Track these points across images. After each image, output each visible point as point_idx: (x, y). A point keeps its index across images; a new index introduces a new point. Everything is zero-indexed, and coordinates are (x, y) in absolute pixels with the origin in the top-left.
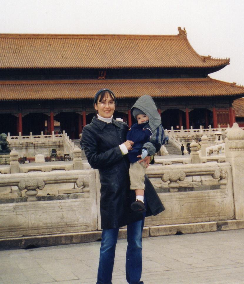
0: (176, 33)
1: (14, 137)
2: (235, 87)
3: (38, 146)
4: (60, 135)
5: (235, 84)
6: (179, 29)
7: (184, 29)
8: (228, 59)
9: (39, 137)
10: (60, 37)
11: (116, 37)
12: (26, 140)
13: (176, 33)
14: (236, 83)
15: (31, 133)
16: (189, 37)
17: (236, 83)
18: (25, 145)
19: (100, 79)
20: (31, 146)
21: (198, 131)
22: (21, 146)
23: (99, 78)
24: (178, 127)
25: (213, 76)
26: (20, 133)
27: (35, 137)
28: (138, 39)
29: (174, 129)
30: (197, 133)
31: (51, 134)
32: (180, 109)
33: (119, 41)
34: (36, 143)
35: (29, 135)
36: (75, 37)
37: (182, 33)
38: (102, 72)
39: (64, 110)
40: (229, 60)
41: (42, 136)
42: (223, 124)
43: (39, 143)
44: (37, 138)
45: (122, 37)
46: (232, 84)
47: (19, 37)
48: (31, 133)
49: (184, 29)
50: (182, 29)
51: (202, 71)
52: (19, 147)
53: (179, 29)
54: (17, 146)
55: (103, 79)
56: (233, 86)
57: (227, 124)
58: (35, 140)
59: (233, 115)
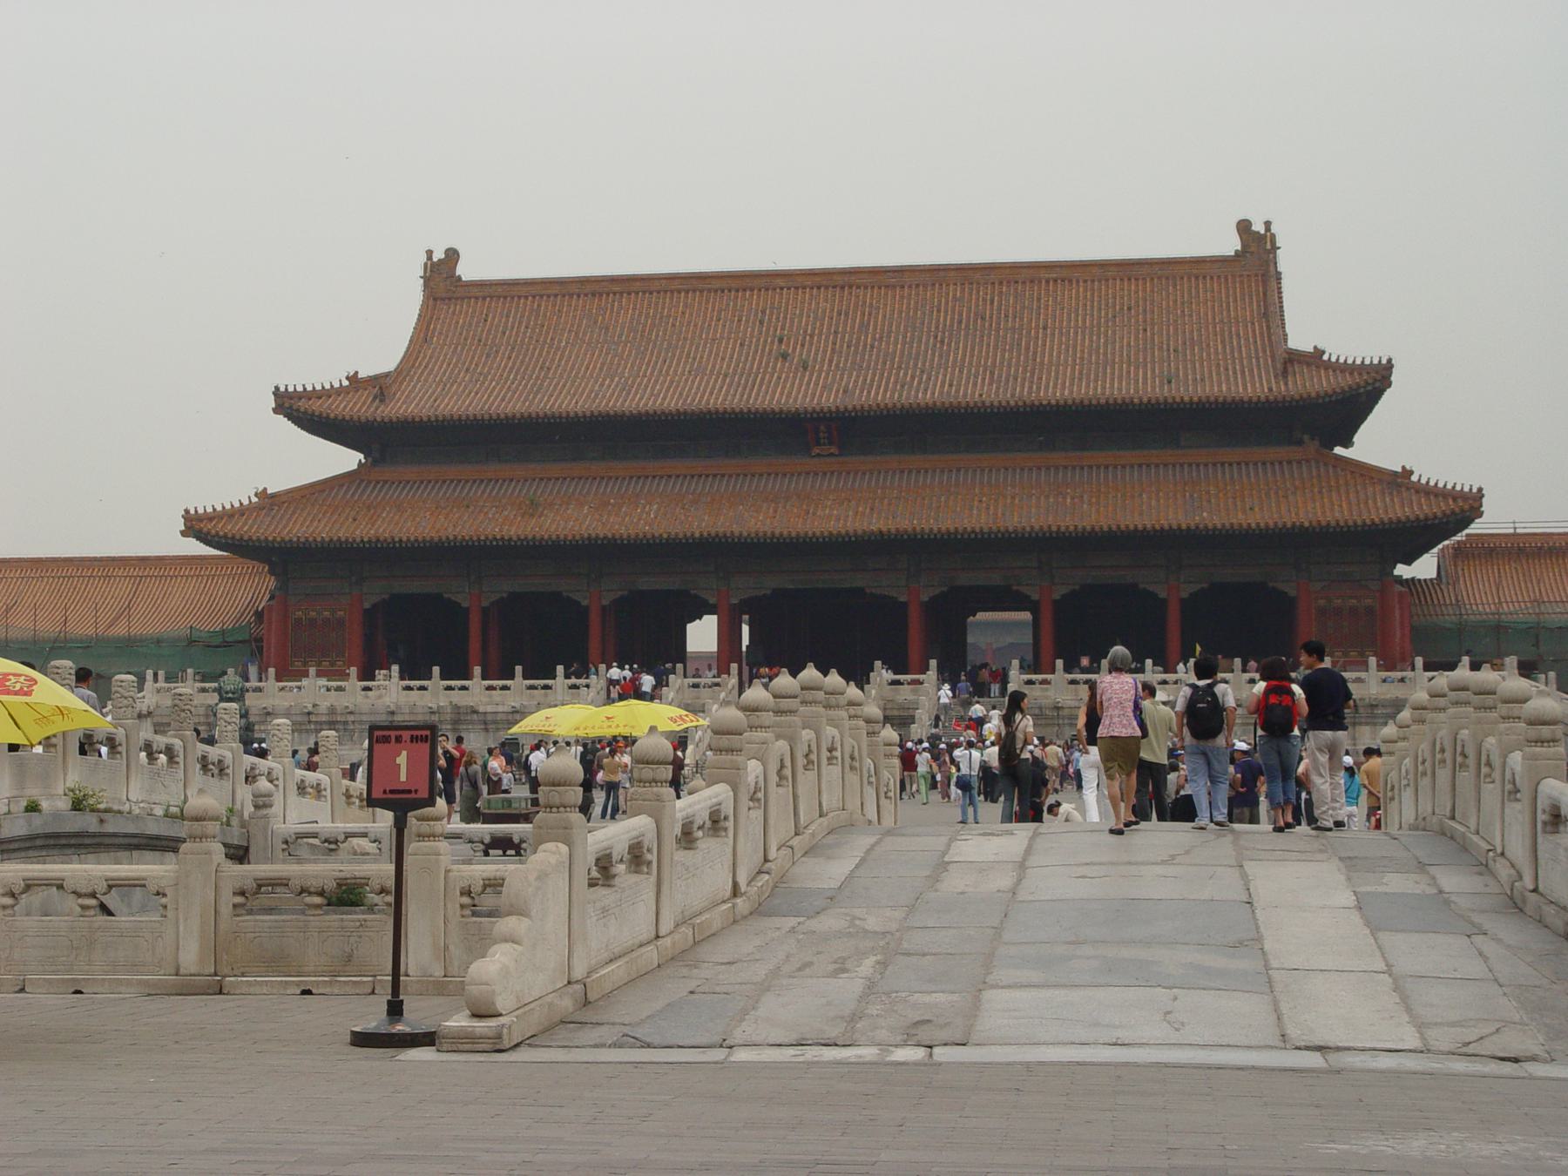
0: (1230, 244)
1: (412, 683)
2: (1408, 489)
3: (495, 722)
6: (1244, 227)
7: (1268, 224)
8: (1384, 361)
10: (717, 284)
11: (952, 274)
12: (457, 698)
13: (1230, 244)
14: (1411, 473)
15: (436, 670)
16: (1286, 262)
18: (448, 717)
19: (818, 455)
20: (472, 722)
23: (816, 450)
24: (1085, 662)
26: (477, 670)
27: (490, 688)
28: (1047, 282)
29: (1068, 669)
32: (1141, 586)
33: (963, 290)
34: (489, 709)
36: (780, 282)
37: (1258, 251)
39: (646, 583)
40: (1389, 366)
41: (518, 682)
42: (1345, 654)
43: (500, 709)
47: (556, 289)
48: (436, 670)
49: (1268, 224)
50: (1258, 227)
53: (1244, 227)
57: (1362, 654)
59: (1397, 613)
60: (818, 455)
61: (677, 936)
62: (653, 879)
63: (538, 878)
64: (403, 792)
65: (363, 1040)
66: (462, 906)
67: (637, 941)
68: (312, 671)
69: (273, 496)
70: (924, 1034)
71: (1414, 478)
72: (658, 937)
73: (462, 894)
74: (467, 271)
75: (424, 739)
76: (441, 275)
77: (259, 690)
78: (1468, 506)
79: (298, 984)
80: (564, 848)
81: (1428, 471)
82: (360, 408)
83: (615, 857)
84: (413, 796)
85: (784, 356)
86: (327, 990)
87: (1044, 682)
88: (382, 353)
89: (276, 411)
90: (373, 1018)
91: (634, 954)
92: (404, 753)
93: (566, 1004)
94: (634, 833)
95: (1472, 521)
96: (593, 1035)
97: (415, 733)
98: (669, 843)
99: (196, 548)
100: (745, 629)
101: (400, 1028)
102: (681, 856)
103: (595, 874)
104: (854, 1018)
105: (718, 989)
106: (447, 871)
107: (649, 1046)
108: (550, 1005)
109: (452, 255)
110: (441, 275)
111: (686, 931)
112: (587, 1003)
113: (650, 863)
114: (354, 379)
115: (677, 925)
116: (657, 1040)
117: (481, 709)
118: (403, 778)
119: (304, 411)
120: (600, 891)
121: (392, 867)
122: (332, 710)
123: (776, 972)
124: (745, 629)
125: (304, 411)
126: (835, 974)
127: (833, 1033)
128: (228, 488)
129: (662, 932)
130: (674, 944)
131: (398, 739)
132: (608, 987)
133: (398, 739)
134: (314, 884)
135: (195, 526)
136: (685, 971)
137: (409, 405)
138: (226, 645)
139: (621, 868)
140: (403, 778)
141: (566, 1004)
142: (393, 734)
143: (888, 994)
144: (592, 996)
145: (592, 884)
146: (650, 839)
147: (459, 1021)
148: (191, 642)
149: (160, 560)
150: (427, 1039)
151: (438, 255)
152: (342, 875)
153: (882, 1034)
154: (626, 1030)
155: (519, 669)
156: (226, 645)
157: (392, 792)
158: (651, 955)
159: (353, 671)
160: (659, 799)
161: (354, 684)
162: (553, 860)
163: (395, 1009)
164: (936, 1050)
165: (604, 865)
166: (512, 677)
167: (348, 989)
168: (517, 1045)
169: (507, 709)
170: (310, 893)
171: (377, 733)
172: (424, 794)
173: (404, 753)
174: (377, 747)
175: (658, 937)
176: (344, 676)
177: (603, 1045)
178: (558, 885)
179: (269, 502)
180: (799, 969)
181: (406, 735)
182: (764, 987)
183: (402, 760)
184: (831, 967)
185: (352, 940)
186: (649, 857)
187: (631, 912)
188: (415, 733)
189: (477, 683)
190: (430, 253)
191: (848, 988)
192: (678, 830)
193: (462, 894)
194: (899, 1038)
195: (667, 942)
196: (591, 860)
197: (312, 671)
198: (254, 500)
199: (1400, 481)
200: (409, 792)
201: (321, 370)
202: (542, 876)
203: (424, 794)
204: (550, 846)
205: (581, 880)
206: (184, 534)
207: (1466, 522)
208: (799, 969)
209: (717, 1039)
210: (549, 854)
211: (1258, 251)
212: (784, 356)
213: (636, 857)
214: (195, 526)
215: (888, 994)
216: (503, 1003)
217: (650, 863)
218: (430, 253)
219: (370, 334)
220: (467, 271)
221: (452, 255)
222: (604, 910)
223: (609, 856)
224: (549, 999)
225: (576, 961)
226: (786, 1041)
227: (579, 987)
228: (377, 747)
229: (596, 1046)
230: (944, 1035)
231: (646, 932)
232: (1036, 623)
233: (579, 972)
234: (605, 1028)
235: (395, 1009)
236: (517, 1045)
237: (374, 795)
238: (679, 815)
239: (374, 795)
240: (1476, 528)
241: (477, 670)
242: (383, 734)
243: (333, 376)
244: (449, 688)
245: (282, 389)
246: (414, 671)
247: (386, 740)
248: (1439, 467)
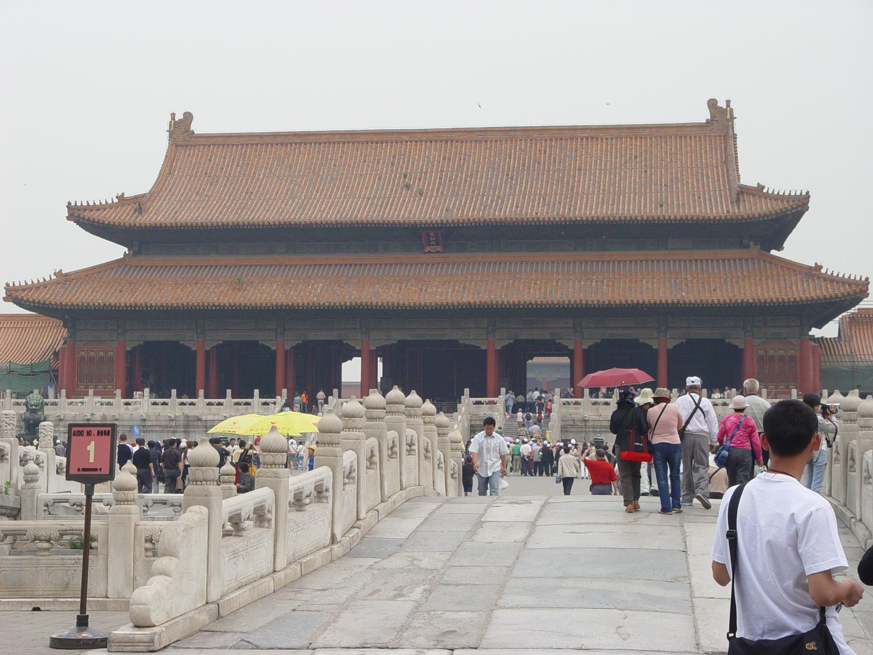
0: (702, 115)
2: (819, 278)
4: (574, 400)
5: (818, 268)
8: (804, 193)
9: (220, 404)
10: (363, 138)
11: (519, 133)
12: (187, 410)
14: (821, 267)
16: (739, 127)
17: (821, 267)
18: (181, 423)
19: (429, 252)
20: (198, 427)
22: (173, 423)
23: (428, 249)
26: (201, 392)
27: (209, 404)
28: (582, 139)
31: (251, 396)
33: (526, 145)
35: (252, 396)
36: (405, 138)
37: (721, 119)
38: (432, 234)
39: (312, 336)
40: (807, 197)
42: (777, 387)
44: (215, 406)
45: (536, 135)
46: (810, 268)
50: (722, 104)
52: (167, 427)
54: (163, 423)
55: (438, 252)
56: (813, 276)
57: (787, 387)
58: (210, 410)
59: (811, 359)
60: (429, 252)
61: (288, 571)
62: (272, 531)
63: (185, 530)
64: (92, 470)
65: (58, 643)
66: (146, 550)
67: (259, 574)
68: (91, 392)
69: (66, 275)
70: (450, 641)
71: (823, 271)
72: (274, 571)
73: (146, 541)
75: (107, 433)
76: (180, 131)
77: (55, 404)
78: (858, 290)
79: (30, 603)
80: (205, 510)
81: (834, 266)
82: (125, 217)
83: (243, 516)
84: (98, 472)
85: (408, 187)
86: (51, 608)
87: (576, 403)
88: (140, 180)
89: (68, 218)
90: (67, 628)
91: (256, 584)
92: (93, 443)
93: (204, 618)
94: (258, 500)
95: (860, 300)
96: (219, 640)
97: (101, 429)
98: (284, 507)
100: (380, 365)
101: (85, 635)
102: (294, 515)
103: (229, 527)
104: (402, 629)
105: (313, 608)
106: (136, 525)
107: (258, 648)
108: (191, 618)
109: (188, 117)
110: (180, 131)
111: (296, 567)
112: (219, 617)
113: (270, 520)
114: (121, 198)
115: (290, 564)
116: (263, 643)
117: (204, 418)
118: (92, 460)
119: (85, 218)
120: (232, 540)
121: (92, 522)
122: (104, 417)
123: (353, 597)
124: (380, 365)
125: (85, 218)
126: (394, 598)
127: (386, 639)
129: (278, 568)
130: (286, 576)
131: (89, 433)
132: (236, 606)
133: (89, 433)
134: (43, 534)
135: (13, 294)
136: (292, 595)
137: (159, 215)
138: (34, 374)
139: (248, 524)
140: (92, 460)
141: (204, 618)
142: (85, 429)
143: (428, 612)
144: (223, 613)
145: (227, 534)
146: (270, 503)
147: (125, 630)
148: (10, 372)
150: (101, 643)
151: (179, 117)
152: (64, 528)
153: (421, 641)
154: (244, 636)
155: (229, 392)
156: (34, 374)
157: (83, 470)
158: (269, 584)
159: (118, 392)
160: (277, 476)
161: (118, 400)
162: (196, 517)
163: (83, 622)
164: (455, 652)
165: (236, 520)
166: (224, 397)
167: (66, 607)
168: (165, 647)
170: (41, 540)
171: (74, 429)
172: (106, 471)
173: (93, 443)
174: (74, 438)
175: (274, 571)
176: (113, 395)
177: (225, 647)
178: (202, 534)
179: (63, 279)
180: (371, 594)
181: (94, 430)
182: (344, 607)
183: (91, 447)
184: (392, 593)
185: (69, 573)
186: (269, 516)
187: (255, 554)
188: (101, 429)
189: (201, 400)
190: (173, 115)
191: (402, 608)
192: (291, 498)
193: (146, 541)
194: (431, 643)
195: (281, 575)
196: (225, 517)
197: (91, 392)
198: (54, 277)
199: (813, 272)
200: (96, 470)
201: (99, 192)
202: (188, 529)
203: (106, 471)
204: (195, 508)
205: (217, 532)
206: (5, 299)
207: (858, 300)
208: (371, 594)
209: (306, 643)
210: (195, 513)
211: (721, 119)
212: (408, 187)
213: (260, 516)
214: (13, 294)
215: (428, 612)
216: (155, 617)
217: (270, 520)
218: (173, 115)
219: (131, 169)
220: (198, 127)
221: (188, 117)
222: (235, 553)
223: (239, 515)
224: (190, 615)
225: (212, 588)
226: (353, 645)
227: (213, 607)
228: (74, 438)
229: (221, 648)
230: (463, 641)
231: (267, 567)
233: (214, 596)
234: (229, 635)
235: (83, 622)
236: (165, 647)
237: (71, 472)
238: (292, 488)
239: (71, 472)
240: (864, 304)
241: (201, 392)
242: (77, 430)
243: (108, 196)
244: (183, 404)
245: (73, 204)
246: (160, 392)
247: (80, 433)
248: (840, 263)
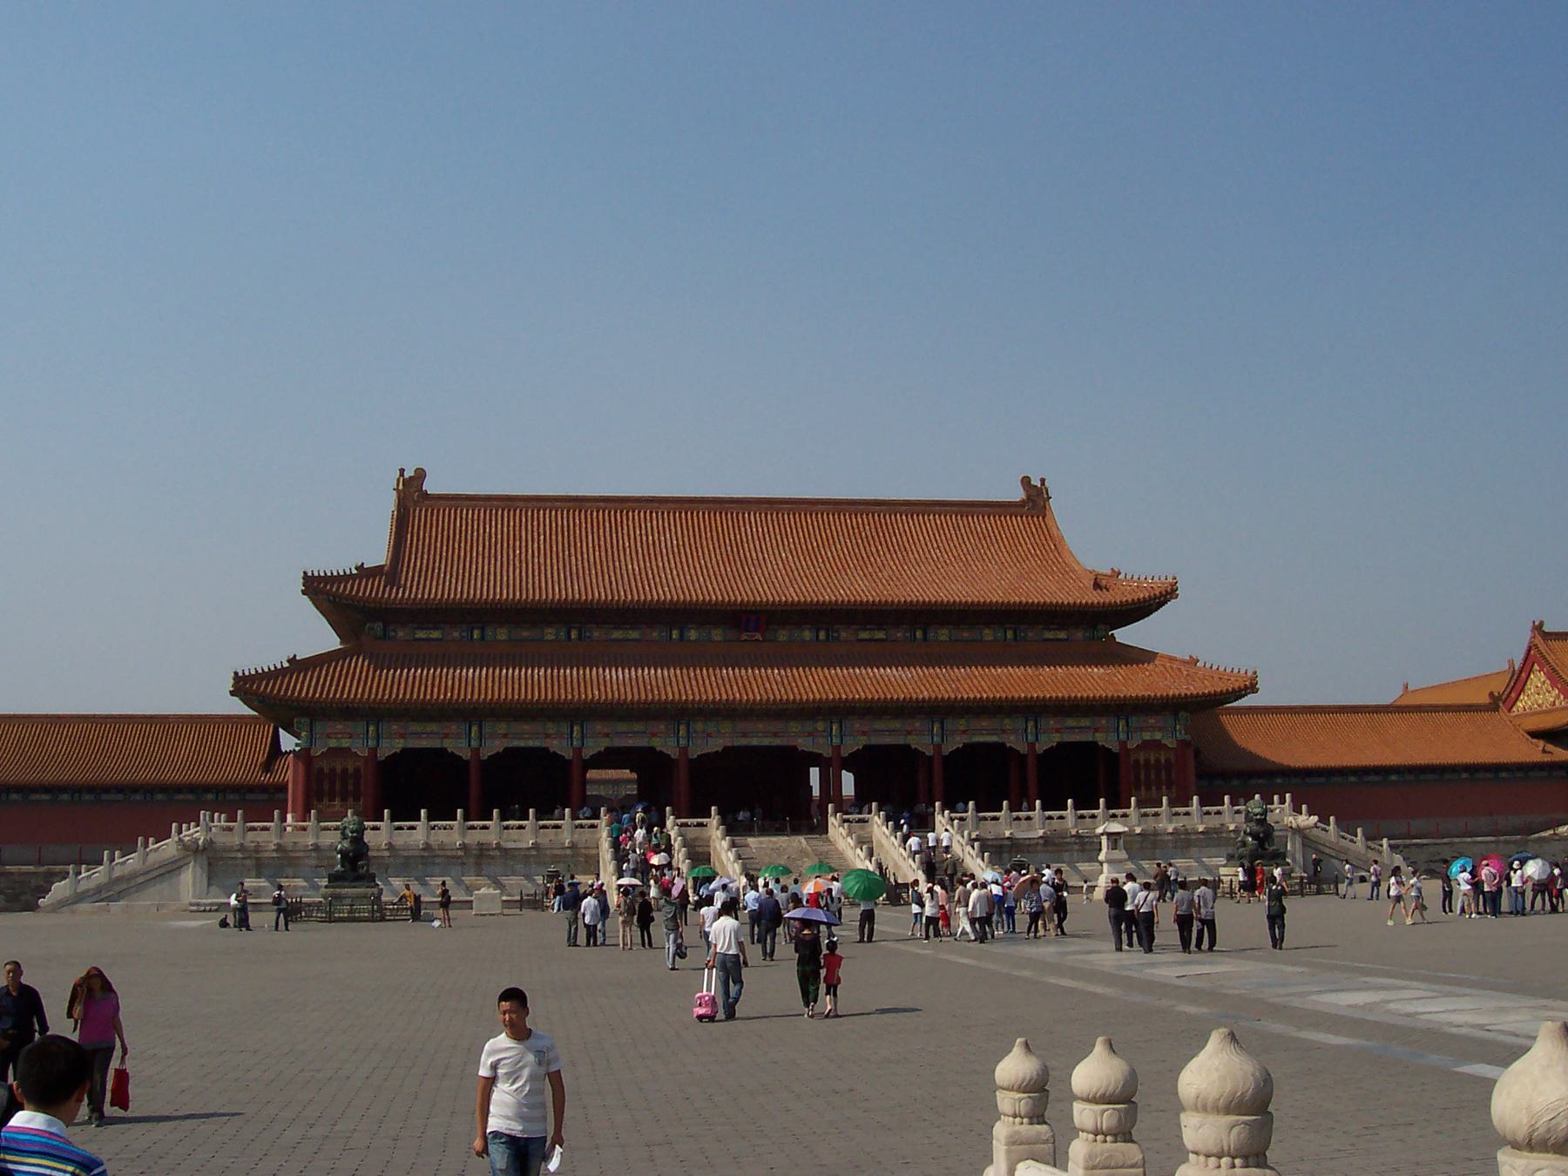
0: (1018, 494)
6: (1026, 481)
7: (1043, 481)
13: (1018, 494)
16: (1059, 506)
21: (1061, 817)
25: (1124, 635)
30: (1056, 824)
37: (1036, 500)
43: (519, 845)
49: (1043, 481)
51: (1092, 624)
53: (1026, 481)
74: (430, 487)
89: (304, 593)
99: (239, 708)
109: (421, 475)
128: (269, 656)
149: (229, 717)
151: (407, 475)
169: (524, 846)
179: (297, 666)
190: (402, 471)
201: (339, 561)
206: (232, 693)
207: (1239, 694)
211: (1036, 500)
214: (244, 686)
218: (402, 471)
220: (430, 487)
221: (421, 475)
232: (584, 782)
240: (1247, 701)
